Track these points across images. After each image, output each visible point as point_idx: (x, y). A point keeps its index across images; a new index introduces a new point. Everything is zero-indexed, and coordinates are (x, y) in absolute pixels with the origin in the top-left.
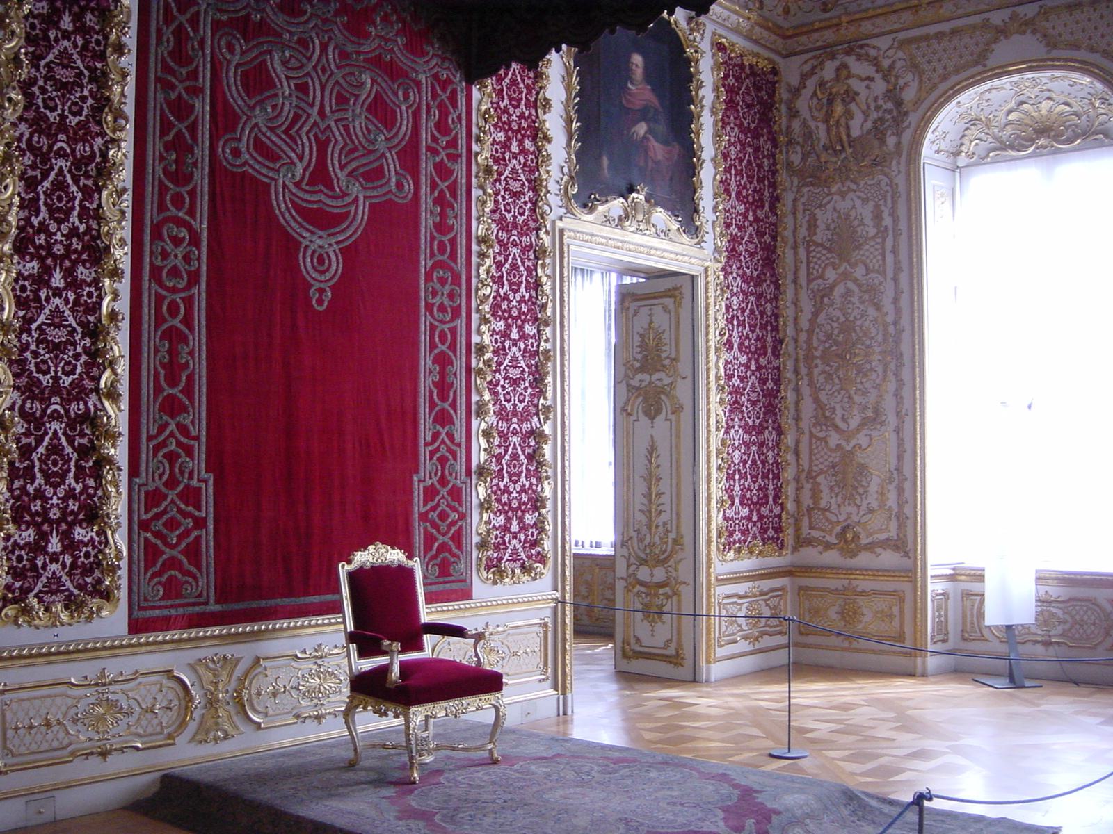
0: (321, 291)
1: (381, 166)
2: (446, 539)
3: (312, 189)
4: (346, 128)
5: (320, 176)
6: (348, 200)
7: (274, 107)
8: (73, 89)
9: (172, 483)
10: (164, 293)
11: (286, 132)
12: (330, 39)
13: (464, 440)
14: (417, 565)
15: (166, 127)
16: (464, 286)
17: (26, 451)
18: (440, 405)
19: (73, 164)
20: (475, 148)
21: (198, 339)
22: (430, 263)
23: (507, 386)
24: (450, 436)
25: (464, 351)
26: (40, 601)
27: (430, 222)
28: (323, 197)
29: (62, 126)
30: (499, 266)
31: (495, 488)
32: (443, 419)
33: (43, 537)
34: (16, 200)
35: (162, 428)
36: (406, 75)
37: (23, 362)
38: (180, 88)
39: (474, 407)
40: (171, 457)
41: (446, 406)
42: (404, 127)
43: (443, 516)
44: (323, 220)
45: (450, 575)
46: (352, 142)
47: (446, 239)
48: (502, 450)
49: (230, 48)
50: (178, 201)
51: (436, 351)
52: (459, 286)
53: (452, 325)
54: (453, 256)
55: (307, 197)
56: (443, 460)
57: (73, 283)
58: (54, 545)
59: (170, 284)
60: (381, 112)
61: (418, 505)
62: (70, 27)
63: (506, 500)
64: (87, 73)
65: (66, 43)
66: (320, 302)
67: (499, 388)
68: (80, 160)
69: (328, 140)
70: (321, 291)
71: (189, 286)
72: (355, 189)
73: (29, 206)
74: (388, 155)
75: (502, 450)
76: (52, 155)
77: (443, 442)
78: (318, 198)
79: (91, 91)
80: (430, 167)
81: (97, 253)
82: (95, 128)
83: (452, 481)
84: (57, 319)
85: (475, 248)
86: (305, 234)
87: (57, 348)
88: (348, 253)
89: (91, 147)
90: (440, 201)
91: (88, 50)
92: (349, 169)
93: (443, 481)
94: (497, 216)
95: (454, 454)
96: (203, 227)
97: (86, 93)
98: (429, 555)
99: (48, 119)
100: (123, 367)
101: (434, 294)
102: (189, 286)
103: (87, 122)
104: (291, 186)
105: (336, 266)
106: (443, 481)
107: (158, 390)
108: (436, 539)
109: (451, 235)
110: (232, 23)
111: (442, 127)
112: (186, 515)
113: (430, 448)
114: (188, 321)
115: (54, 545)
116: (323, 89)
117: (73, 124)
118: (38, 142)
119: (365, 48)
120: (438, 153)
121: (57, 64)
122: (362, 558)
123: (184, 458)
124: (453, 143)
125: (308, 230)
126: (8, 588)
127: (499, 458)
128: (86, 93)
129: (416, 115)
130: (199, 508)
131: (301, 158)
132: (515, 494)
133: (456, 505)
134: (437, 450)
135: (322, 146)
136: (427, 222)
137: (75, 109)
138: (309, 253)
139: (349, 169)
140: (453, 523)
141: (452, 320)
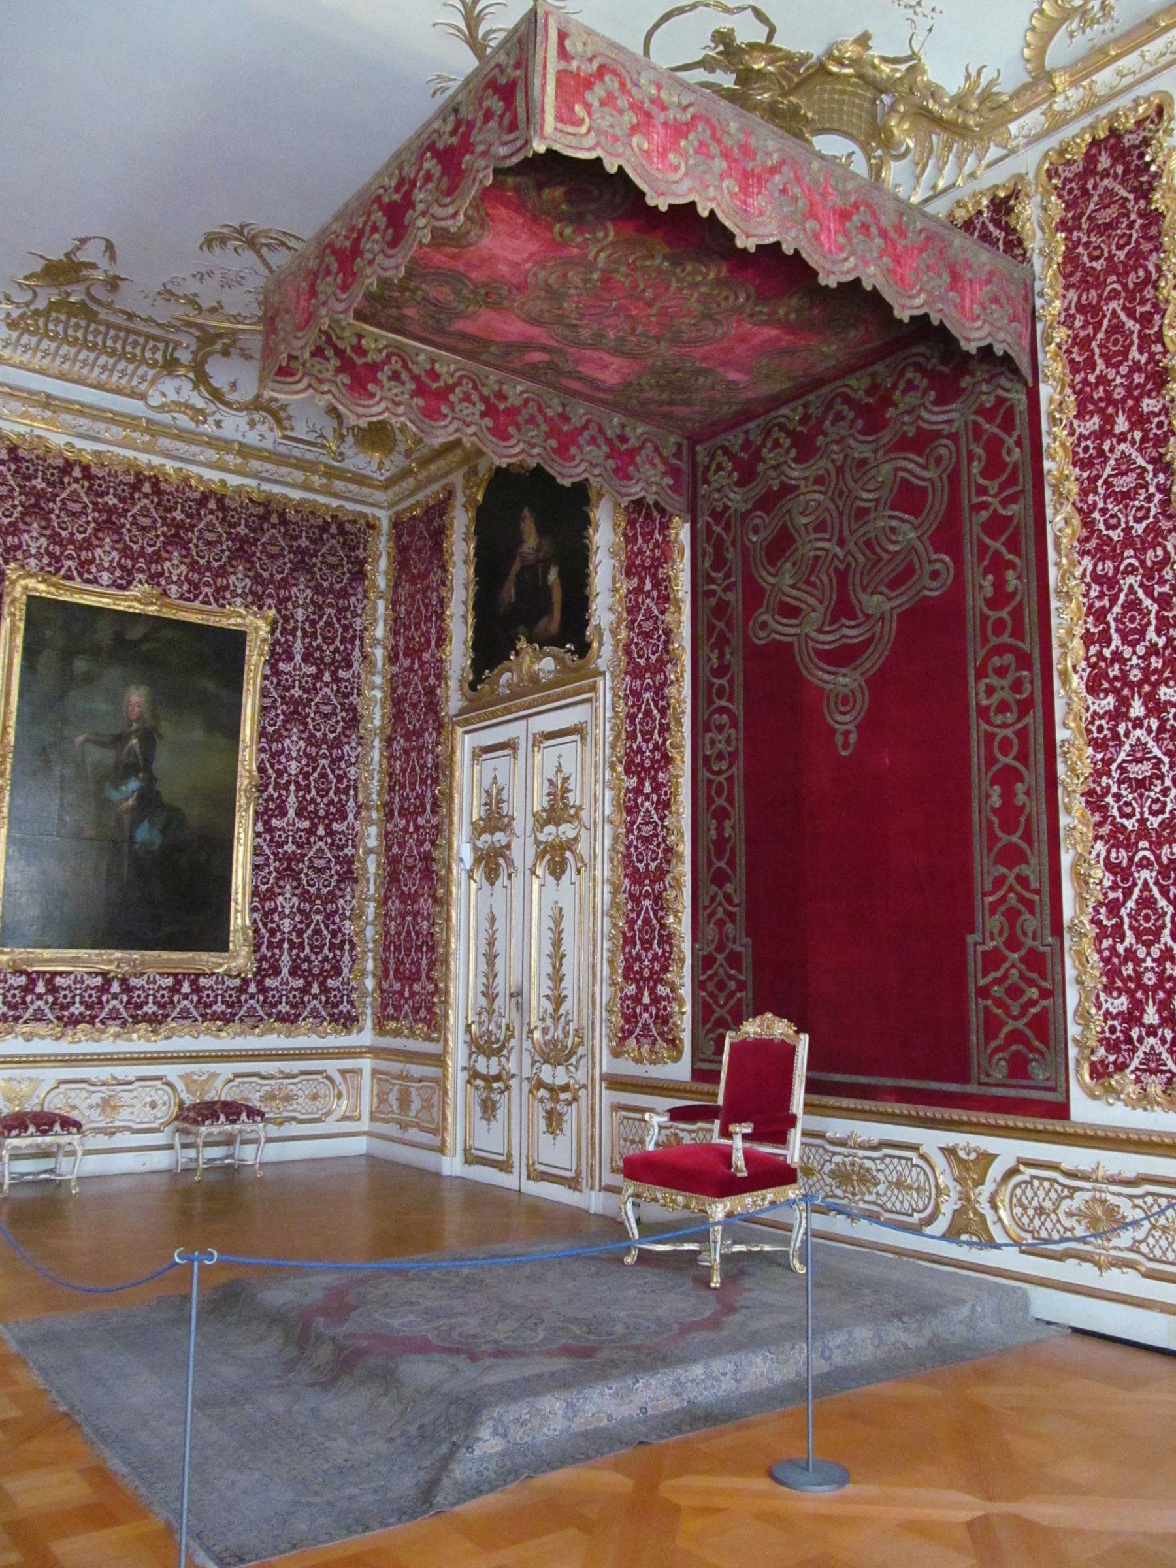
0: (846, 734)
1: (911, 564)
2: (1020, 1024)
3: (834, 627)
4: (868, 543)
5: (843, 609)
6: (872, 621)
7: (794, 564)
9: (720, 948)
10: (712, 777)
11: (807, 582)
12: (846, 457)
13: (1046, 881)
14: (803, 1044)
15: (711, 628)
16: (1037, 666)
17: (631, 923)
18: (1005, 839)
20: (1047, 465)
21: (738, 813)
22: (982, 653)
23: (1124, 793)
24: (1023, 881)
25: (1041, 756)
26: (638, 1042)
27: (980, 603)
28: (846, 631)
30: (1100, 615)
31: (1106, 953)
32: (1012, 856)
34: (624, 735)
35: (713, 899)
36: (938, 434)
37: (629, 855)
38: (720, 592)
39: (1062, 833)
40: (720, 924)
41: (1015, 838)
42: (938, 503)
43: (1014, 992)
44: (842, 656)
45: (1027, 1076)
46: (873, 551)
47: (1004, 614)
48: (1119, 894)
49: (756, 531)
50: (721, 693)
51: (995, 769)
52: (1029, 668)
53: (1019, 725)
54: (1018, 633)
55: (829, 638)
56: (1012, 915)
59: (715, 768)
60: (909, 498)
61: (976, 979)
63: (1131, 972)
66: (846, 746)
67: (1109, 799)
69: (849, 565)
70: (846, 734)
71: (730, 766)
72: (874, 603)
73: (631, 736)
74: (918, 544)
75: (1119, 894)
77: (1011, 889)
78: (852, 633)
80: (976, 529)
81: (667, 759)
83: (1029, 942)
85: (1054, 604)
86: (827, 677)
88: (877, 684)
90: (998, 567)
92: (872, 586)
93: (1013, 944)
94: (1092, 544)
95: (1030, 906)
96: (738, 708)
98: (993, 1044)
100: (686, 849)
101: (990, 691)
102: (730, 766)
104: (814, 634)
105: (863, 701)
106: (1013, 944)
107: (710, 863)
108: (1003, 1024)
109: (1014, 604)
110: (754, 509)
111: (994, 466)
112: (731, 977)
113: (990, 899)
114: (730, 800)
116: (841, 514)
119: (882, 443)
120: (984, 506)
122: (751, 1028)
123: (729, 925)
124: (1012, 480)
125: (829, 673)
126: (622, 1029)
127: (1114, 908)
129: (954, 478)
130: (740, 972)
131: (821, 602)
132: (1149, 963)
133: (1034, 976)
134: (1003, 899)
135: (842, 577)
136: (976, 601)
138: (832, 699)
139: (872, 586)
140: (1032, 1003)
141: (1019, 719)
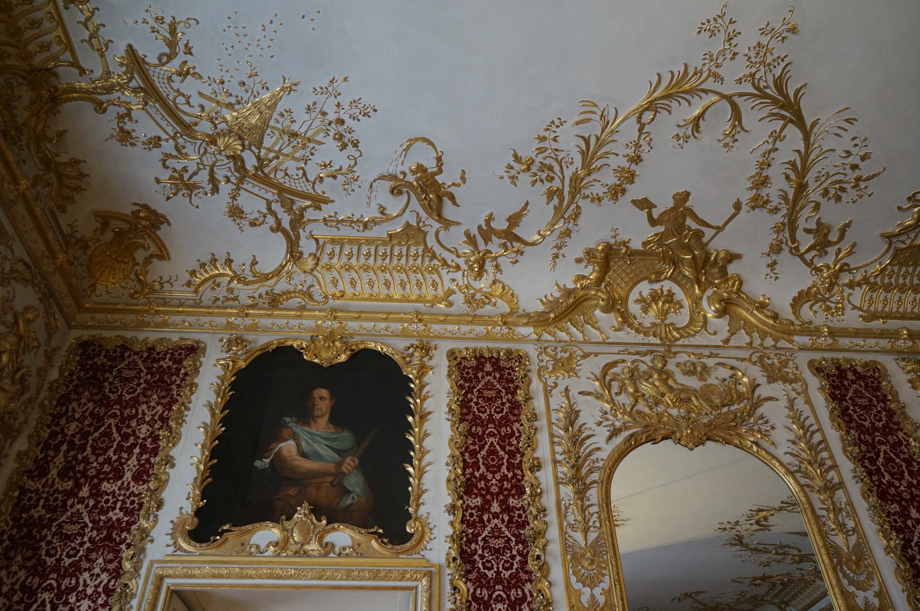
8: (504, 552)
19: (509, 605)
29: (498, 579)
62: (498, 510)
64: (513, 539)
65: (496, 521)
68: (515, 602)
76: (492, 601)
79: (518, 551)
82: (524, 577)
89: (523, 591)
91: (512, 523)
97: (514, 552)
99: (487, 576)
103: (518, 572)
117: (507, 576)
118: (481, 594)
121: (491, 537)
128: (514, 552)
137: (507, 565)
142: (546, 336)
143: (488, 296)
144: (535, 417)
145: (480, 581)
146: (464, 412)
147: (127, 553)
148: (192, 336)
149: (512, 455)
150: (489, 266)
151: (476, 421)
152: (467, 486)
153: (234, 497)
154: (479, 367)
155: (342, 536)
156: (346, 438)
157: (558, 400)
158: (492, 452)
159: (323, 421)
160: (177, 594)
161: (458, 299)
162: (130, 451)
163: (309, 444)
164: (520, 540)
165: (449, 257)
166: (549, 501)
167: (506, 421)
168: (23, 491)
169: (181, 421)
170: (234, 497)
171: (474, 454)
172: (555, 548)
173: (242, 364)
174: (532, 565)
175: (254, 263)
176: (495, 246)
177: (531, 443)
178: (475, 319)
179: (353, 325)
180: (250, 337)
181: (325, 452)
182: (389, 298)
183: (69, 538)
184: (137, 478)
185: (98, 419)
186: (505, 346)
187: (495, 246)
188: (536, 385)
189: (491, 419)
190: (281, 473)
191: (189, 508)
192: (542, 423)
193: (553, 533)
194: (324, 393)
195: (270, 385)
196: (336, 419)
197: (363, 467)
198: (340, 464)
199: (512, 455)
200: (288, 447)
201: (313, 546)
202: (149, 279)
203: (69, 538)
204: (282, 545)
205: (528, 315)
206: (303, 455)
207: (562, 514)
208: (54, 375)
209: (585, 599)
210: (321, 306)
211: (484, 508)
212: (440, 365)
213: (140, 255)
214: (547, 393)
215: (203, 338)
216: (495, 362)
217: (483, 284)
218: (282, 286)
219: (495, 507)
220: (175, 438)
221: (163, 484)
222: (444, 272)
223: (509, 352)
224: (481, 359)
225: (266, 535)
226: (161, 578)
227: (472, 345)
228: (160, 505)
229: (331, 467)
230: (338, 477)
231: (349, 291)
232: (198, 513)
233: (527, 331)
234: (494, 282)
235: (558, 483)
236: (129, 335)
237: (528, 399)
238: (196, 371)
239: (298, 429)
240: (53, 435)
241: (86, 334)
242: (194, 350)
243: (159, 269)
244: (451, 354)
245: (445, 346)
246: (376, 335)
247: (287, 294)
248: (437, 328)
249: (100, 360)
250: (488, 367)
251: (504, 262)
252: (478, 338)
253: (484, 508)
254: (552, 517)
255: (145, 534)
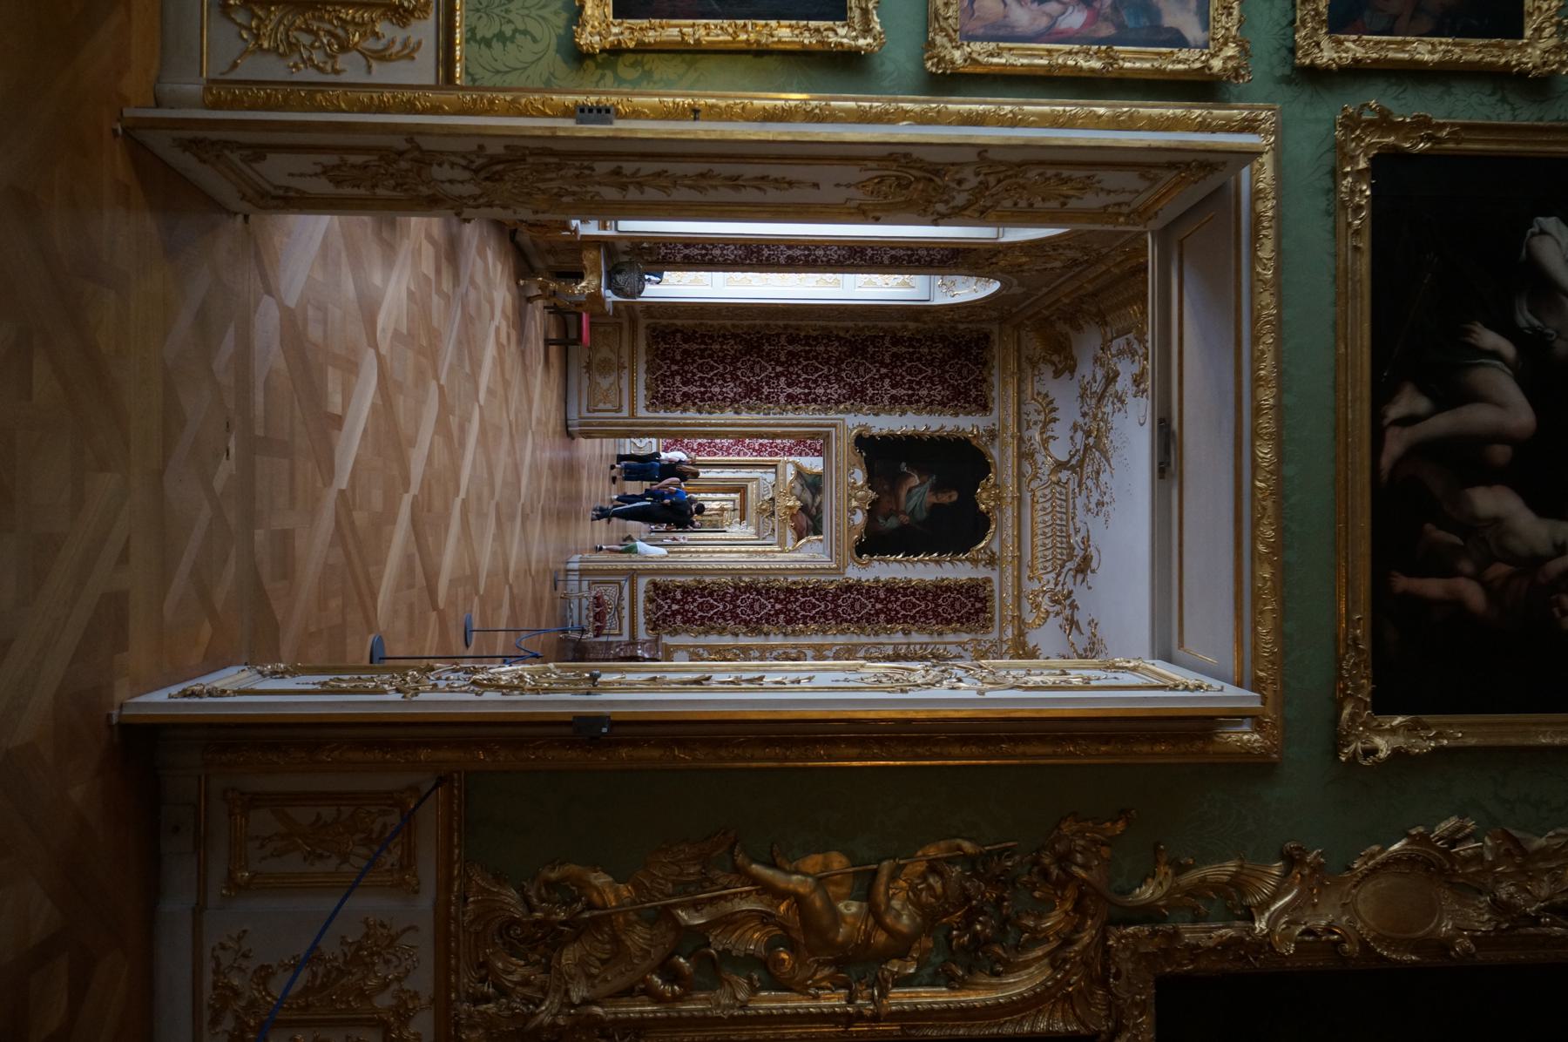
33: (678, 602)
57: (777, 613)
58: (675, 607)
84: (763, 607)
87: (751, 606)
115: (675, 607)
142: (1005, 647)
143: (1038, 606)
144: (940, 634)
145: (836, 596)
146: (940, 590)
147: (848, 404)
148: (996, 406)
149: (913, 617)
150: (1058, 608)
151: (936, 596)
152: (891, 589)
153: (880, 455)
154: (977, 599)
155: (859, 518)
156: (922, 515)
157: (953, 650)
158: (915, 605)
159: (934, 500)
160: (828, 435)
161: (1036, 586)
162: (911, 388)
163: (917, 493)
164: (860, 619)
165: (1061, 579)
166: (883, 638)
167: (936, 615)
168: (883, 338)
169: (931, 412)
170: (880, 455)
171: (913, 594)
172: (855, 640)
173: (974, 442)
174: (845, 625)
175: (1055, 439)
176: (1068, 612)
177: (921, 630)
178: (1018, 598)
179: (1009, 513)
180: (997, 443)
181: (912, 504)
182: (1034, 535)
183: (856, 371)
184: (893, 397)
185: (930, 364)
186: (997, 617)
187: (1068, 612)
188: (965, 637)
189: (938, 606)
190: (897, 479)
191: (875, 431)
192: (936, 639)
193: (863, 639)
194: (955, 498)
195: (961, 463)
196: (935, 508)
197: (903, 528)
198: (904, 513)
199: (913, 617)
200: (915, 480)
201: (854, 503)
202: (1041, 365)
203: (856, 371)
204: (853, 486)
205: (1021, 634)
206: (910, 490)
207: (874, 645)
208: (961, 327)
209: (826, 653)
210: (1024, 488)
211: (878, 599)
212: (980, 573)
213: (1055, 358)
214: (959, 644)
215: (995, 413)
216: (983, 610)
217: (1045, 603)
218: (1039, 458)
219: (879, 606)
220: (918, 412)
221: (890, 412)
222: (1053, 575)
223: (991, 620)
224: (984, 600)
225: (859, 476)
226: (834, 426)
227: (997, 594)
228: (877, 415)
229: (902, 507)
230: (896, 513)
231: (1038, 507)
232: (872, 437)
233: (1009, 633)
234: (1047, 612)
235: (895, 645)
236: (996, 363)
237: (955, 631)
238: (969, 413)
239: (927, 485)
240: (919, 341)
241: (995, 337)
242: (985, 408)
243: (1048, 371)
244: (988, 580)
245: (994, 576)
246: (1000, 528)
247: (1034, 464)
248: (1009, 572)
249: (975, 351)
250: (978, 605)
251: (1060, 619)
252: (1001, 598)
253: (878, 599)
254: (873, 639)
255: (859, 410)
